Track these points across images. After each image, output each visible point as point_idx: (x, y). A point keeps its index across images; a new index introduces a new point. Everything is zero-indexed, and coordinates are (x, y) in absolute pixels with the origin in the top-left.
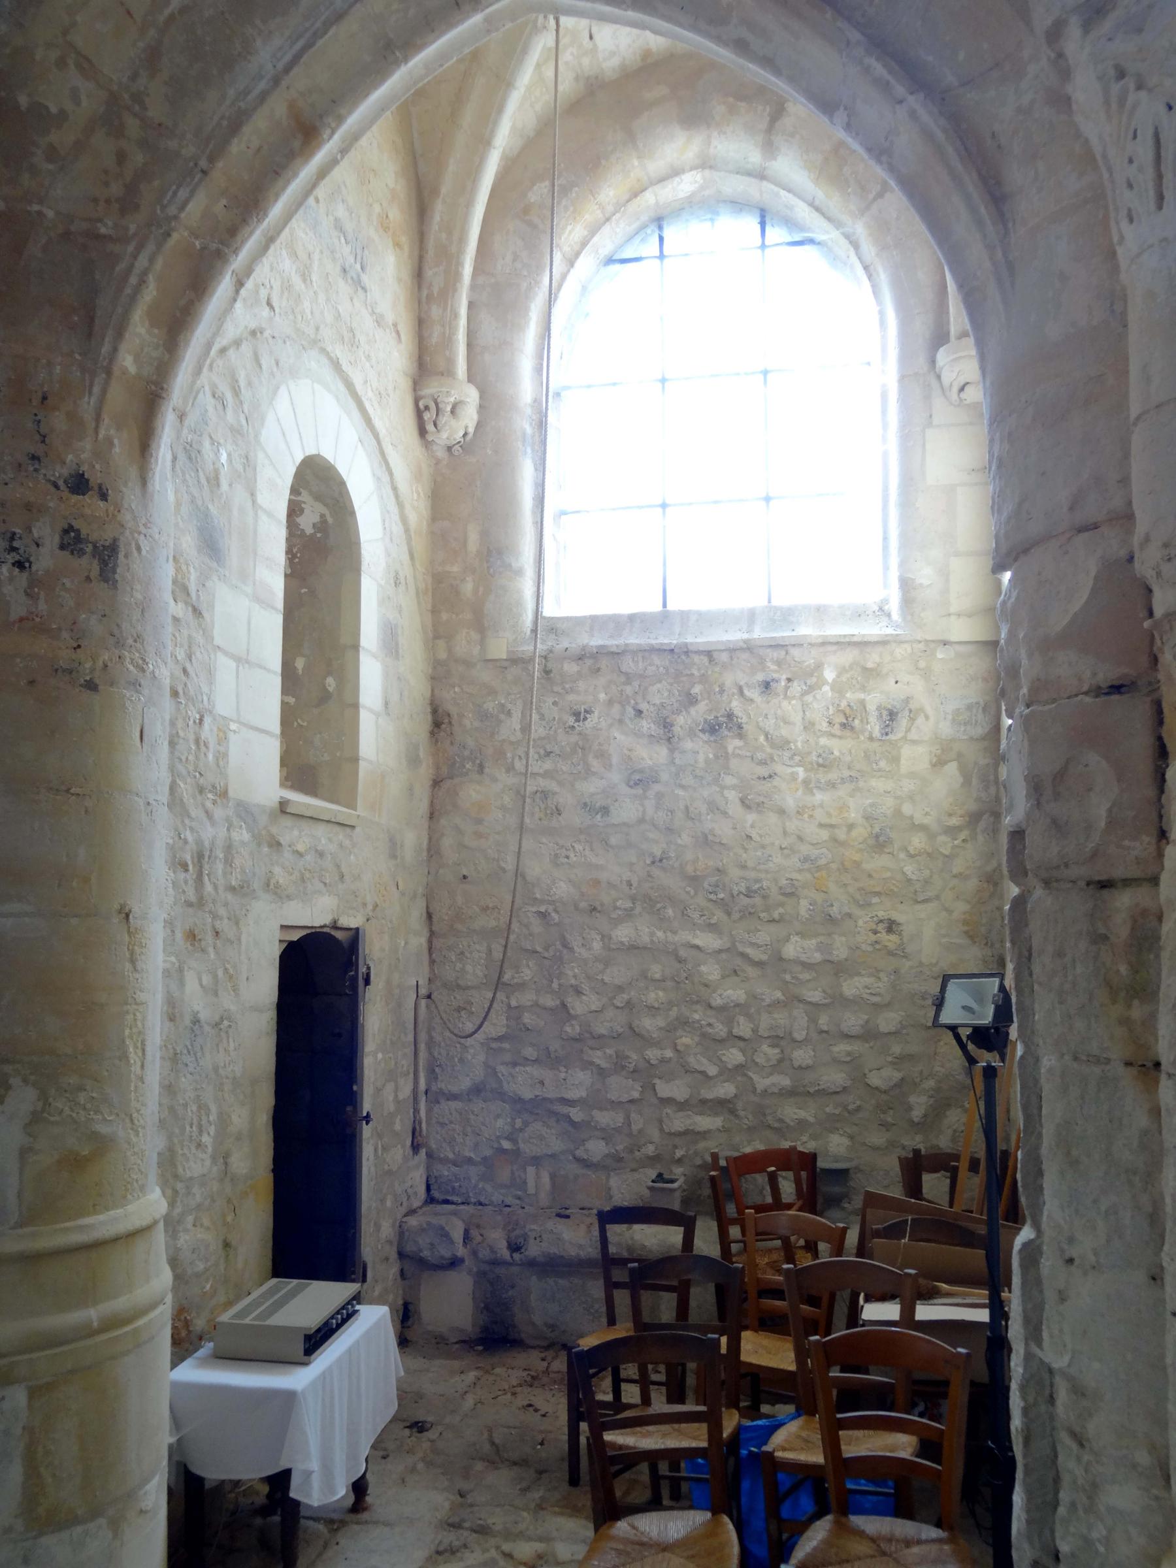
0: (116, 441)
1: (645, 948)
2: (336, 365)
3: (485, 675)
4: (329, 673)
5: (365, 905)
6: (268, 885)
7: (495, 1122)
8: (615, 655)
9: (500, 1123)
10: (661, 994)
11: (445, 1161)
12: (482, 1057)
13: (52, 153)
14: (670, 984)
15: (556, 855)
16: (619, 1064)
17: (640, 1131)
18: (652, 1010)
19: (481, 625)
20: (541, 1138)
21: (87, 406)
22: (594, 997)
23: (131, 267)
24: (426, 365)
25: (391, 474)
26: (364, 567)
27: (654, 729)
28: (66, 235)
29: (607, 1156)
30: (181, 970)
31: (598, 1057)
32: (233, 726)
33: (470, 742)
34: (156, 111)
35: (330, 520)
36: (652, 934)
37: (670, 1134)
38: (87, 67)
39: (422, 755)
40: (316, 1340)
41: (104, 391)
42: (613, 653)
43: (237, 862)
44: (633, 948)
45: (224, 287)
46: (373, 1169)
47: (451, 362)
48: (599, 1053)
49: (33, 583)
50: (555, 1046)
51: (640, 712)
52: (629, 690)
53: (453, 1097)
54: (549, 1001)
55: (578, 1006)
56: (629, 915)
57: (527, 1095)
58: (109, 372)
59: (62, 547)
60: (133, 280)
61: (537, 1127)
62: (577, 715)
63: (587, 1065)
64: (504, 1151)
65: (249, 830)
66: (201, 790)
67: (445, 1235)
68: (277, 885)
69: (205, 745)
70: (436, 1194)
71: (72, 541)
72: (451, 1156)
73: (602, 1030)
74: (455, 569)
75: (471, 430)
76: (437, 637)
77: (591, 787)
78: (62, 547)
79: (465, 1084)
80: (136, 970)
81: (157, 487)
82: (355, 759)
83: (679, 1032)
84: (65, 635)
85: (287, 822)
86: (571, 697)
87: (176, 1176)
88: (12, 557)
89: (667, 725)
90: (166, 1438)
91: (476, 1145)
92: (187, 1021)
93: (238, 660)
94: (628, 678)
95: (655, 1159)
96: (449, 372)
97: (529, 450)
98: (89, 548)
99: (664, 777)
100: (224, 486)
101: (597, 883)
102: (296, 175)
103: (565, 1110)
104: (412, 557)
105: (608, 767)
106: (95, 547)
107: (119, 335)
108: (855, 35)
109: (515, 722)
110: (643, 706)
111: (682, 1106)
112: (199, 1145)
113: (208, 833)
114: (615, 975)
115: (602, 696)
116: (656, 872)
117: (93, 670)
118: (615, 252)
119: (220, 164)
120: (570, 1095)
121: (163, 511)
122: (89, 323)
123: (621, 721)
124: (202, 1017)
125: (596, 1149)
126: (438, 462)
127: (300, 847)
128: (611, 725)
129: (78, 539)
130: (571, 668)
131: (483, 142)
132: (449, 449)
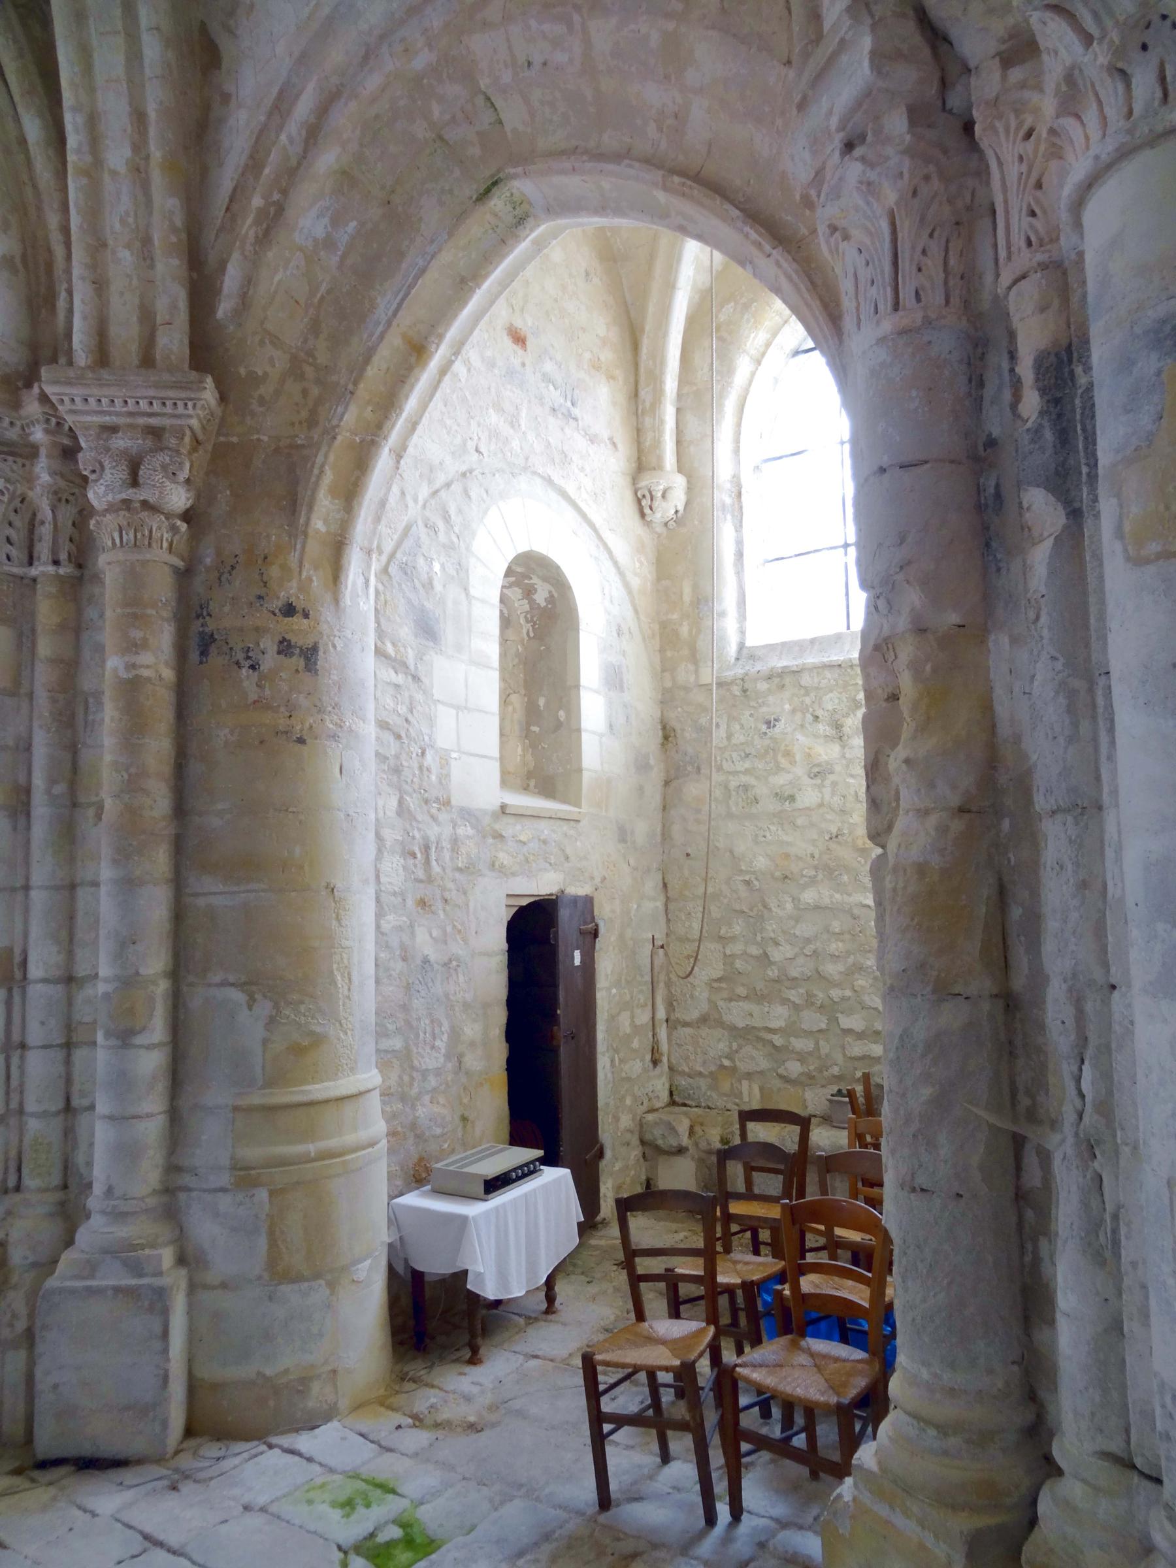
0: (314, 578)
1: (826, 908)
2: (549, 481)
3: (699, 697)
4: (560, 708)
5: (592, 878)
6: (493, 865)
7: (717, 1044)
8: (796, 673)
9: (721, 1045)
10: (840, 944)
11: (683, 1073)
12: (705, 995)
13: (262, 401)
14: (847, 936)
15: (756, 835)
16: (809, 1000)
17: (827, 1055)
18: (835, 958)
19: (694, 658)
20: (752, 1058)
21: (293, 560)
22: (788, 947)
23: (314, 463)
24: (642, 464)
25: (610, 552)
26: (582, 626)
27: (829, 731)
28: (277, 450)
29: (802, 1074)
30: (412, 926)
31: (793, 995)
32: (454, 755)
33: (690, 750)
34: (322, 358)
35: (556, 595)
36: (831, 897)
37: (851, 1058)
38: (276, 341)
39: (652, 762)
40: (495, 1184)
41: (303, 547)
42: (794, 672)
43: (463, 850)
44: (817, 907)
45: (383, 461)
46: (609, 1075)
47: (660, 458)
48: (793, 992)
49: (260, 680)
50: (760, 985)
51: (817, 717)
52: (808, 700)
53: (686, 1024)
54: (754, 951)
55: (776, 955)
56: (813, 881)
57: (741, 1025)
58: (305, 534)
59: (279, 653)
60: (316, 471)
61: (748, 1049)
62: (768, 723)
63: (785, 1001)
64: (725, 1067)
65: (473, 827)
66: (426, 802)
67: (673, 1129)
68: (502, 866)
69: (429, 770)
70: (677, 1099)
71: (285, 647)
72: (687, 1070)
73: (794, 973)
74: (675, 616)
75: (681, 508)
76: (663, 671)
77: (780, 780)
78: (279, 653)
79: (694, 1015)
80: (341, 925)
81: (349, 603)
82: (580, 770)
83: (856, 976)
84: (282, 709)
85: (506, 820)
86: (764, 709)
87: (413, 1068)
88: (248, 663)
89: (838, 726)
90: (384, 1236)
91: (704, 1062)
92: (419, 962)
93: (458, 708)
94: (807, 691)
95: (839, 1078)
96: (659, 467)
97: (729, 517)
98: (297, 651)
99: (838, 768)
100: (438, 587)
101: (787, 856)
102: (417, 380)
103: (769, 1036)
104: (636, 611)
105: (793, 763)
106: (301, 650)
107: (310, 509)
108: (736, 213)
109: (722, 732)
110: (820, 713)
111: (860, 1036)
112: (433, 1047)
113: (433, 832)
114: (804, 929)
115: (787, 707)
116: (833, 846)
117: (301, 730)
118: (800, 345)
119: (362, 386)
120: (775, 1024)
121: (359, 616)
122: (293, 502)
123: (802, 726)
124: (432, 958)
125: (794, 1068)
126: (659, 536)
127: (523, 838)
128: (795, 730)
129: (289, 645)
130: (763, 686)
131: (670, 287)
132: (666, 524)
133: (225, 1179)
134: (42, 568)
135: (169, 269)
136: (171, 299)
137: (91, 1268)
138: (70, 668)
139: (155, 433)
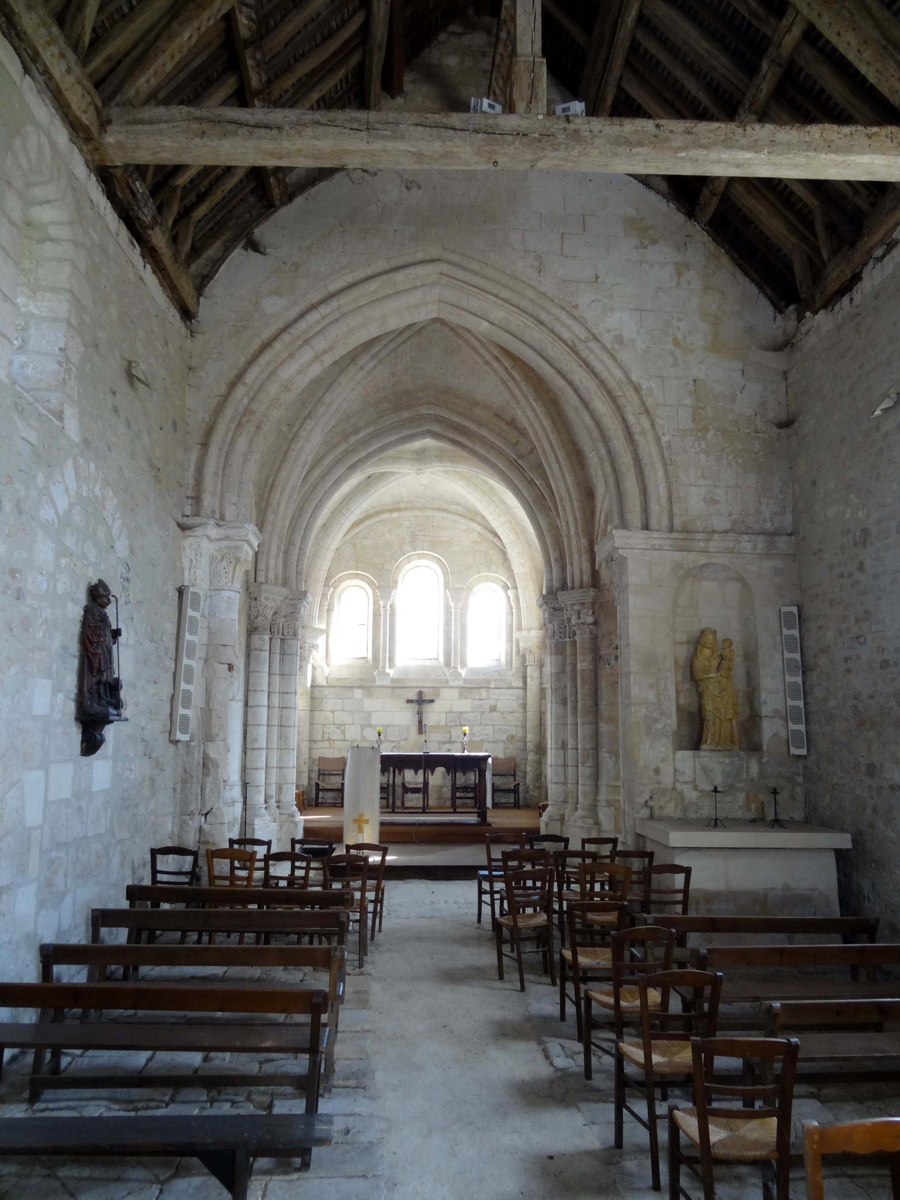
133: (603, 803)
134: (567, 639)
135: (585, 557)
136: (586, 566)
137: (576, 821)
138: (574, 665)
139: (583, 604)
